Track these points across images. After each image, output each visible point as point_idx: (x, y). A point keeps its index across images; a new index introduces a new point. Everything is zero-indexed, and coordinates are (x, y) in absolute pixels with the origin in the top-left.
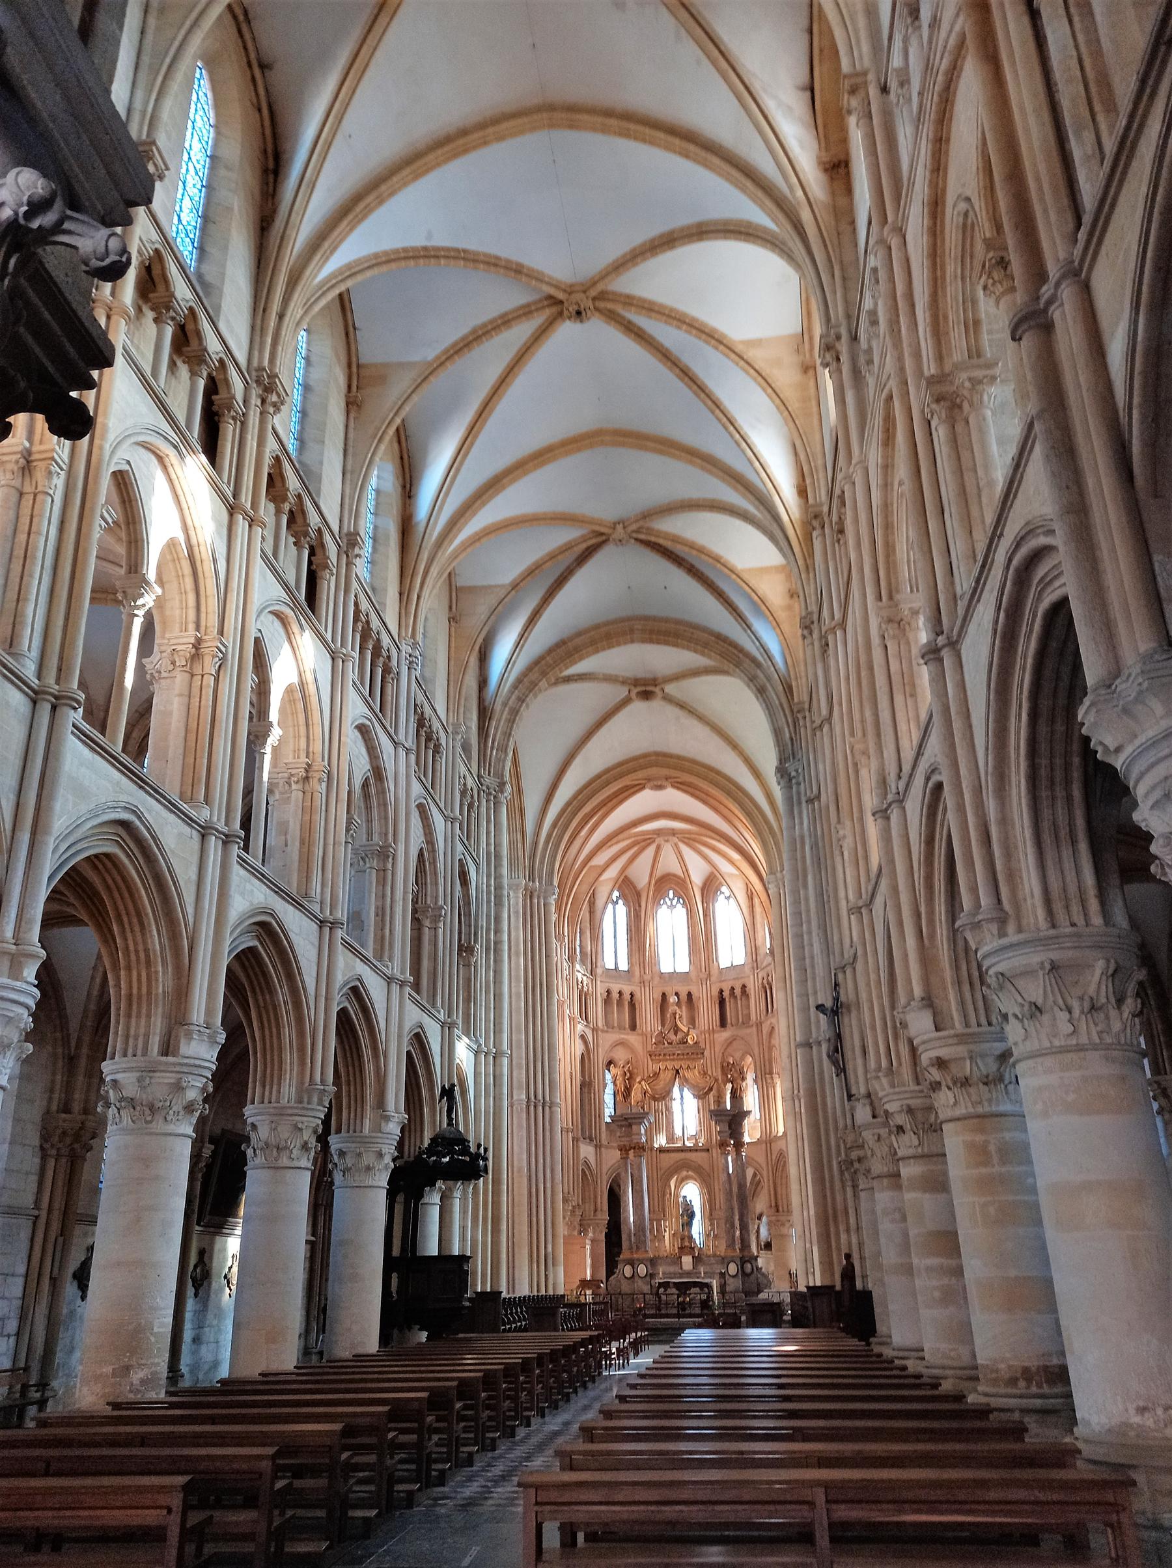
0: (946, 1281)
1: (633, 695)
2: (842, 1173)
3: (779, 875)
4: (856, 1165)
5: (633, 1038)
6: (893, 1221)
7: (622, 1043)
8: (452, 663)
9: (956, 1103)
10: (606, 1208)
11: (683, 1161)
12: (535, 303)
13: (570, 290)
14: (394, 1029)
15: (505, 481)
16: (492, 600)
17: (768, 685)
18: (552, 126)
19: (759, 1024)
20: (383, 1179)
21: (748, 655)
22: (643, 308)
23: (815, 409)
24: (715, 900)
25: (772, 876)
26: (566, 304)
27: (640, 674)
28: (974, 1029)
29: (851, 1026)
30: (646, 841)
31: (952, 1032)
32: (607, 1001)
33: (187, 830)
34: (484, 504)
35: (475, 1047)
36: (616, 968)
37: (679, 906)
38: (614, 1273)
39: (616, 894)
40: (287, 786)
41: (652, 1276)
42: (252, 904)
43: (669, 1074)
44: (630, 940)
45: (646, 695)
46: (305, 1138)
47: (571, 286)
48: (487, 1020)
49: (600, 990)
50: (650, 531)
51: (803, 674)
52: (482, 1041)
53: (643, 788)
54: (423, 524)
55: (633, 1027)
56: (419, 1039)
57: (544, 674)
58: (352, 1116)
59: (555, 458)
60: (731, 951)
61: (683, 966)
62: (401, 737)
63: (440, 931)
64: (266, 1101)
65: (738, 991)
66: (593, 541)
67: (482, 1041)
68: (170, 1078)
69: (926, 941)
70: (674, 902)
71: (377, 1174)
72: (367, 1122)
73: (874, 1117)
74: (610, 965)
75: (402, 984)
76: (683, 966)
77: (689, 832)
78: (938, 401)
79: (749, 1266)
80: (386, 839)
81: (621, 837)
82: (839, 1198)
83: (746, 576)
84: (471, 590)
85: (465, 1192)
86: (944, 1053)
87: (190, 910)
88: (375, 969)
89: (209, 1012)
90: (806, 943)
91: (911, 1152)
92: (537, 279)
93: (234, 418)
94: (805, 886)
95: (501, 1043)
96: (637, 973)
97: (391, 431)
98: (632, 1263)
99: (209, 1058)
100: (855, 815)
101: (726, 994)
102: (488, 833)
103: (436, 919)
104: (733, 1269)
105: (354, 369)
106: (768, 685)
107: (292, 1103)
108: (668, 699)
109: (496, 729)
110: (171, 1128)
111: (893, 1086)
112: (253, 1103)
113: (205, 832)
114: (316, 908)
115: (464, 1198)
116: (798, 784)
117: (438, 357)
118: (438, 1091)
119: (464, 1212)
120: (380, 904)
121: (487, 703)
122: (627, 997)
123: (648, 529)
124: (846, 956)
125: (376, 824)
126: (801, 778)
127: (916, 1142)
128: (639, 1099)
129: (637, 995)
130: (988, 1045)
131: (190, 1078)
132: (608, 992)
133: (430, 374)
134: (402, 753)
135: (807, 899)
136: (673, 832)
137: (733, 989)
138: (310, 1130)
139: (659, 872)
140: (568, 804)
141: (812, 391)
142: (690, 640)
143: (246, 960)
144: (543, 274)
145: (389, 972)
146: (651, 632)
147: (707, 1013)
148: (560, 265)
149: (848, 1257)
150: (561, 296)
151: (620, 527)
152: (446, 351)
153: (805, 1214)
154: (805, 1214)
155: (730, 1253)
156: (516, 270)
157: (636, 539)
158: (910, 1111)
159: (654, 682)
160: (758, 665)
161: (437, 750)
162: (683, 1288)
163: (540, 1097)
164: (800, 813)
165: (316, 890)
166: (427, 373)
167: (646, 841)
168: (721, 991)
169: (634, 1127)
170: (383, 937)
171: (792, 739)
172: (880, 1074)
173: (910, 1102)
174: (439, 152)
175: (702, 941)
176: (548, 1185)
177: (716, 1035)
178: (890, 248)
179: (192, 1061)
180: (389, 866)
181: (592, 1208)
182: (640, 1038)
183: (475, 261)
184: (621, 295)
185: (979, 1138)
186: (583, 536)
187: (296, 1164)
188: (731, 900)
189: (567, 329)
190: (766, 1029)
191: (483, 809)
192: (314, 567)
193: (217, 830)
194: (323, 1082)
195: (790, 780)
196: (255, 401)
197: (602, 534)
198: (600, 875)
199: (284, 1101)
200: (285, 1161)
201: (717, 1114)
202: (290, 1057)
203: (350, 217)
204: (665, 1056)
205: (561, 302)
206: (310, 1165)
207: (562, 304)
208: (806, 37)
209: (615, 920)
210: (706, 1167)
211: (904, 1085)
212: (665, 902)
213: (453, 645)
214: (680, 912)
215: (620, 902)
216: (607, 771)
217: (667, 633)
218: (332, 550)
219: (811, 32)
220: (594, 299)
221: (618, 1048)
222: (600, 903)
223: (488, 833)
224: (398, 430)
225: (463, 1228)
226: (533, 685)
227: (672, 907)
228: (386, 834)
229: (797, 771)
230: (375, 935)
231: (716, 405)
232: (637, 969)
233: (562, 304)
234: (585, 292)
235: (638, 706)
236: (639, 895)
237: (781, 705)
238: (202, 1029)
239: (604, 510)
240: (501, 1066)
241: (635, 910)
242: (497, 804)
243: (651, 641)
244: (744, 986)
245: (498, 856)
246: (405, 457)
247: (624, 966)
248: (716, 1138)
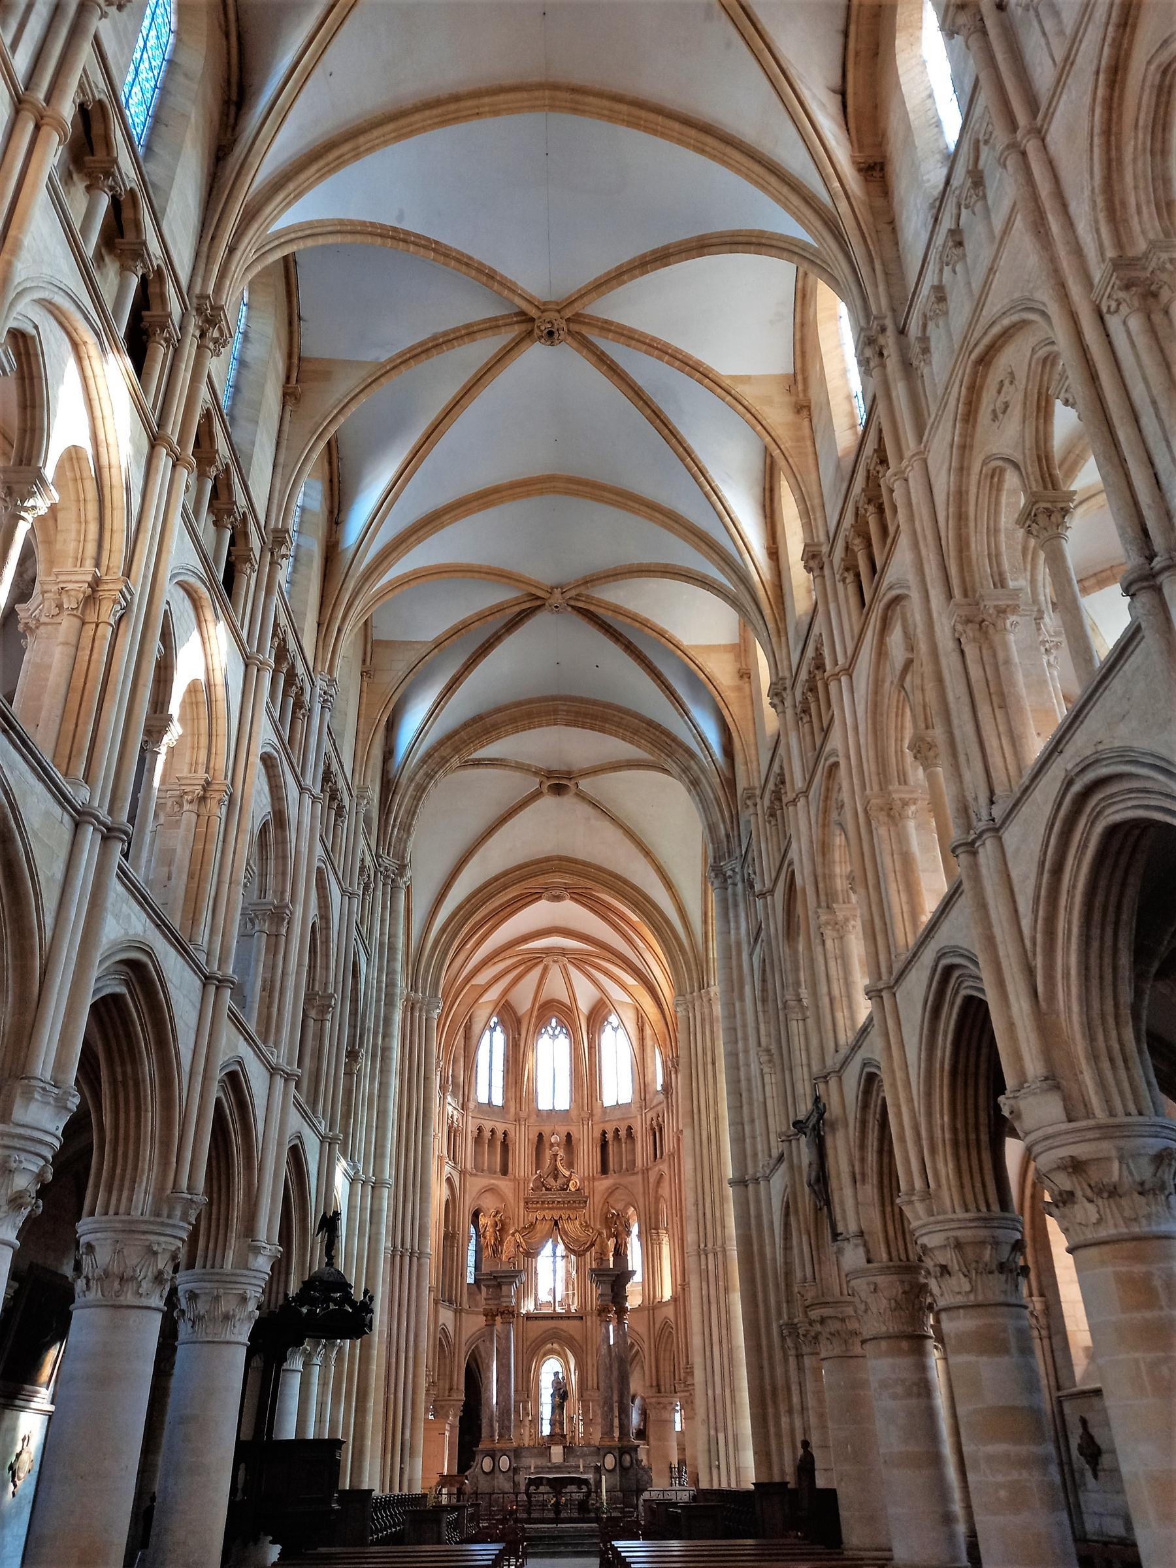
0: (1015, 1475)
1: (545, 788)
2: (783, 1338)
3: (688, 997)
4: (818, 1327)
5: (504, 1185)
6: (895, 1397)
7: (491, 1190)
8: (362, 720)
9: (1100, 1221)
10: (462, 1386)
11: (552, 1331)
12: (503, 317)
13: (543, 308)
14: (274, 1134)
15: (445, 518)
16: (413, 657)
17: (702, 777)
18: (552, 107)
19: (646, 1171)
20: (243, 1332)
21: (681, 744)
22: (622, 335)
23: (810, 449)
24: (601, 1029)
25: (681, 998)
26: (537, 323)
27: (555, 767)
28: (1121, 1119)
29: (835, 1148)
30: (534, 960)
31: (1091, 1122)
32: (478, 1140)
33: (57, 810)
34: (419, 541)
35: (352, 1173)
36: (490, 1103)
37: (562, 1036)
38: (469, 1467)
39: (495, 1019)
40: (176, 808)
41: (516, 1470)
42: (127, 934)
43: (547, 1226)
44: (506, 1072)
45: (558, 790)
46: (160, 1266)
47: (545, 303)
48: (368, 1142)
49: (471, 1127)
50: (589, 599)
51: (754, 758)
52: (360, 1167)
53: (540, 898)
54: (349, 555)
55: (505, 1171)
56: (296, 1155)
57: (457, 750)
58: (211, 1246)
59: (502, 501)
60: (617, 1087)
61: (563, 1103)
62: (308, 781)
63: (328, 1025)
64: (111, 1212)
65: (623, 1133)
66: (528, 605)
67: (360, 1167)
69: (1043, 1004)
70: (557, 1032)
72: (230, 1254)
73: (869, 1261)
74: (483, 1098)
75: (288, 1077)
76: (563, 1103)
77: (581, 952)
78: (1127, 287)
79: (628, 1458)
80: (282, 899)
81: (509, 953)
82: (779, 1370)
83: (692, 653)
84: (388, 644)
85: (326, 1358)
86: (1081, 1151)
87: (49, 920)
88: (260, 1054)
89: (60, 1065)
90: (741, 1063)
91: (959, 1300)
92: (510, 289)
93: (167, 340)
94: (742, 998)
95: (382, 1171)
96: (512, 1110)
97: (322, 445)
98: (493, 1454)
99: (52, 1129)
100: (871, 882)
101: (609, 1136)
102: (383, 921)
104: (610, 1461)
105: (296, 361)
106: (702, 777)
107: (146, 1217)
108: (582, 796)
109: (400, 804)
111: (931, 1213)
112: (92, 1214)
113: (80, 817)
114: (202, 958)
115: (325, 1366)
116: (735, 884)
117: (391, 360)
118: (313, 1222)
119: (324, 1384)
121: (391, 776)
122: (500, 1136)
123: (588, 596)
124: (829, 1062)
125: (271, 881)
126: (738, 877)
127: (967, 1288)
128: (511, 1254)
129: (511, 1134)
130: (1140, 1141)
131: (23, 1156)
132: (480, 1129)
133: (382, 375)
134: (308, 801)
135: (743, 1013)
136: (563, 952)
137: (617, 1130)
138: (167, 1256)
139: (544, 996)
140: (460, 908)
141: (807, 431)
142: (619, 725)
143: (107, 1011)
144: (515, 284)
145: (273, 1060)
146: (577, 713)
147: (587, 1156)
148: (536, 277)
149: (806, 1444)
150: (533, 312)
151: (557, 592)
152: (402, 354)
153: (710, 1393)
154: (710, 1393)
155: (607, 1443)
156: (488, 276)
157: (573, 607)
158: (959, 1245)
159: (569, 775)
160: (692, 755)
161: (339, 814)
162: (558, 1485)
163: (408, 1246)
164: (737, 916)
165: (203, 937)
166: (379, 374)
167: (534, 960)
168: (604, 1133)
169: (504, 1288)
170: (269, 1017)
171: (728, 836)
172: (914, 1198)
173: (958, 1233)
174: (427, 113)
175: (586, 1076)
176: (411, 1354)
177: (596, 1183)
178: (1024, 154)
180: (284, 931)
181: (447, 1387)
182: (511, 1184)
183: (446, 256)
184: (598, 319)
185: (1139, 1269)
186: (516, 598)
187: (145, 1302)
188: (621, 1031)
189: (536, 354)
190: (652, 1178)
191: (379, 893)
193: (97, 818)
194: (190, 1189)
195: (726, 881)
196: (192, 330)
197: (538, 598)
198: (481, 995)
199: (136, 1214)
200: (129, 1298)
201: (599, 1274)
202: (149, 1152)
203: (321, 163)
204: (544, 1204)
205: (532, 320)
206: (161, 1304)
207: (535, 323)
208: (839, 39)
209: (492, 1048)
210: (578, 1337)
211: (945, 1213)
212: (546, 1031)
213: (364, 700)
214: (563, 1044)
215: (498, 1029)
216: (505, 874)
217: (594, 717)
219: (846, 34)
220: (568, 320)
221: (486, 1194)
222: (477, 1027)
224: (329, 443)
225: (321, 1405)
226: (445, 760)
227: (554, 1036)
228: (283, 892)
229: (733, 870)
230: (260, 1014)
231: (685, 453)
232: (512, 1104)
233: (535, 323)
234: (559, 311)
235: (548, 802)
236: (519, 1021)
237: (717, 799)
238: (48, 1087)
239: (542, 571)
240: (381, 1198)
241: (514, 1038)
242: (395, 888)
243: (575, 724)
245: (392, 948)
246: (336, 480)
247: (498, 1100)
248: (594, 1302)
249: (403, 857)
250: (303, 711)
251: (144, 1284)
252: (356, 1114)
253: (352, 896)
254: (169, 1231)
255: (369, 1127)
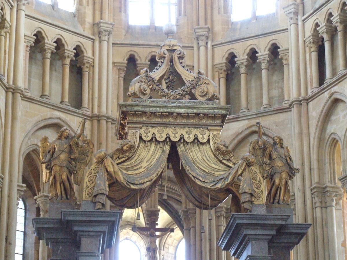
49: (26, 29)
55: (77, 102)
101: (242, 58)
129: (88, 53)
132: (39, 38)
137: (253, 54)
168: (232, 59)
244: (274, 50)
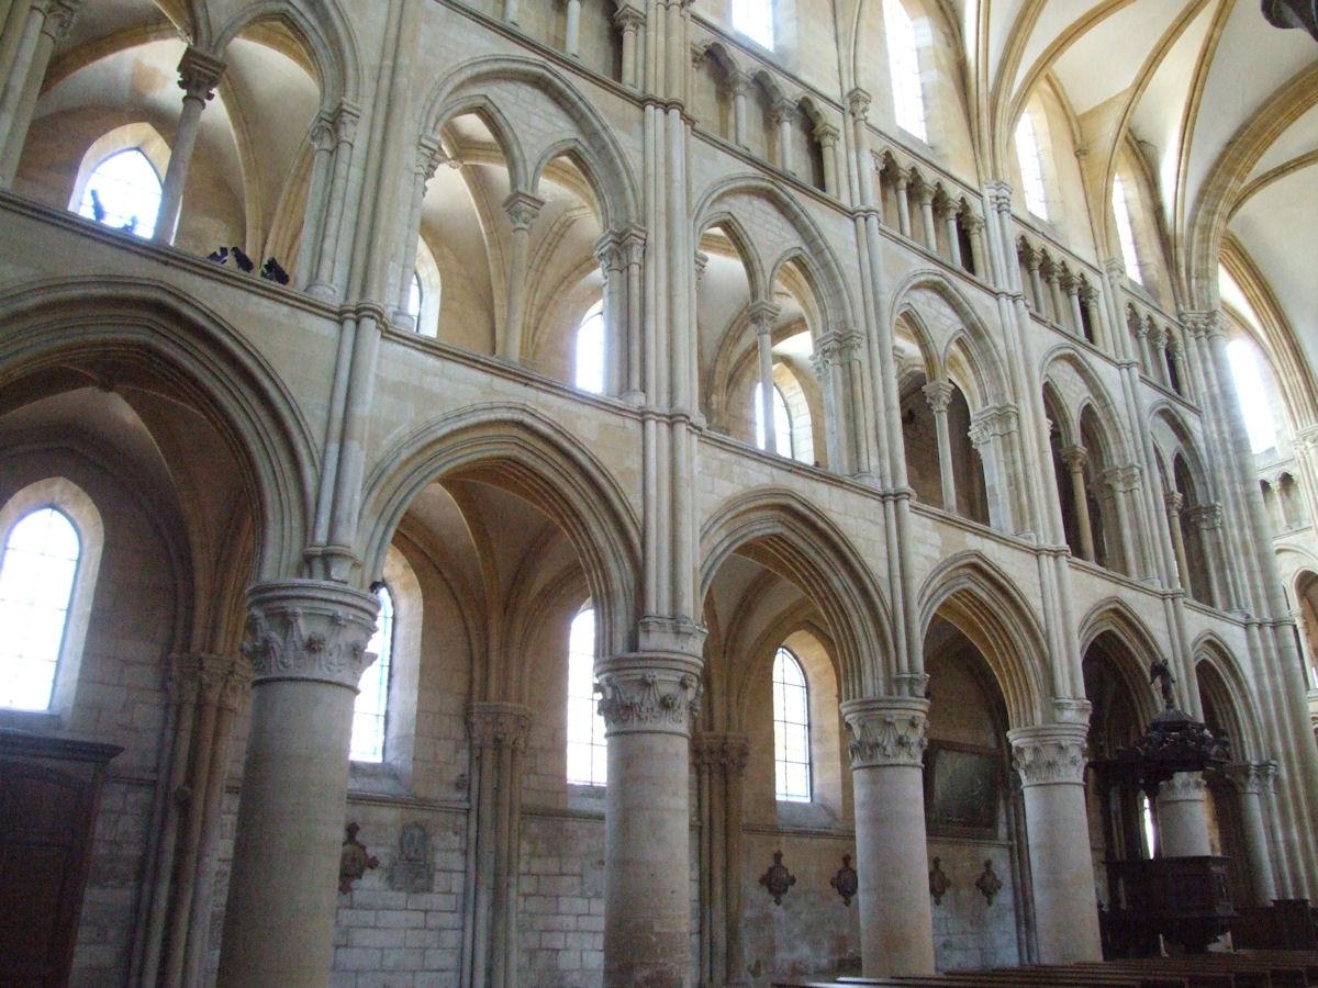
8: (1090, 198)
35: (1243, 620)
48: (1254, 587)
62: (1003, 286)
63: (1138, 495)
68: (637, 674)
71: (1062, 769)
72: (1038, 715)
75: (1056, 554)
84: (1095, 112)
85: (1264, 787)
102: (1206, 374)
103: (1129, 480)
110: (647, 726)
115: (1263, 795)
119: (1268, 810)
120: (1011, 471)
145: (1034, 544)
179: (654, 655)
187: (893, 761)
191: (1193, 349)
192: (816, 139)
194: (912, 669)
200: (880, 760)
213: (1086, 178)
218: (832, 118)
223: (1206, 374)
225: (1271, 829)
249: (1210, 304)
250: (977, 225)
251: (889, 748)
252: (1230, 564)
253: (1129, 366)
254: (898, 705)
255: (1251, 572)
